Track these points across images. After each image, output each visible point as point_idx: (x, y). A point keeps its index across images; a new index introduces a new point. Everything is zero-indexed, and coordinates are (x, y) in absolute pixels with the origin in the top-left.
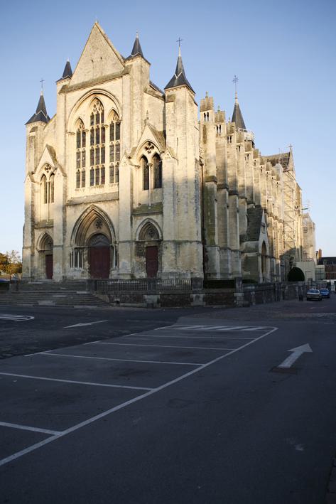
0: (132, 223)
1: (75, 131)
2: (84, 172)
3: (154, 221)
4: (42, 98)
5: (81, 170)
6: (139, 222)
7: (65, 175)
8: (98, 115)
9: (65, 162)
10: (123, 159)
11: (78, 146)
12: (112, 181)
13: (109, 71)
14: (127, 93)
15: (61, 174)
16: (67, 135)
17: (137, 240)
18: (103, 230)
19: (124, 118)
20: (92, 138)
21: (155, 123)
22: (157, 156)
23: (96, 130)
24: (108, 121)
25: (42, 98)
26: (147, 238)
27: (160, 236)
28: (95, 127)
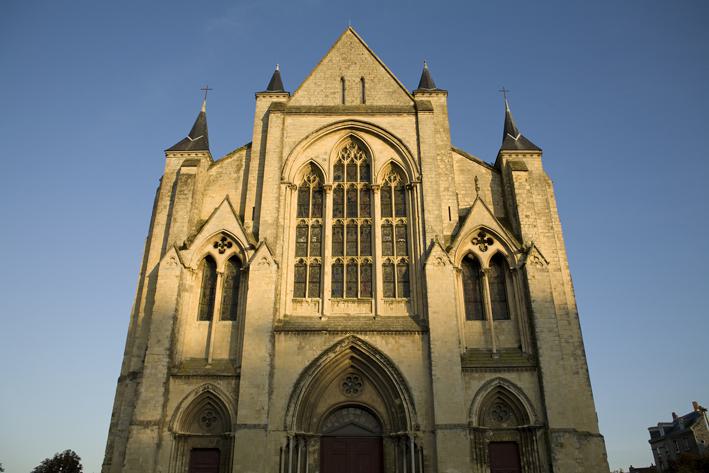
1: (298, 183)
3: (515, 386)
5: (309, 260)
8: (352, 165)
9: (276, 237)
11: (302, 211)
16: (283, 186)
17: (475, 425)
26: (491, 423)
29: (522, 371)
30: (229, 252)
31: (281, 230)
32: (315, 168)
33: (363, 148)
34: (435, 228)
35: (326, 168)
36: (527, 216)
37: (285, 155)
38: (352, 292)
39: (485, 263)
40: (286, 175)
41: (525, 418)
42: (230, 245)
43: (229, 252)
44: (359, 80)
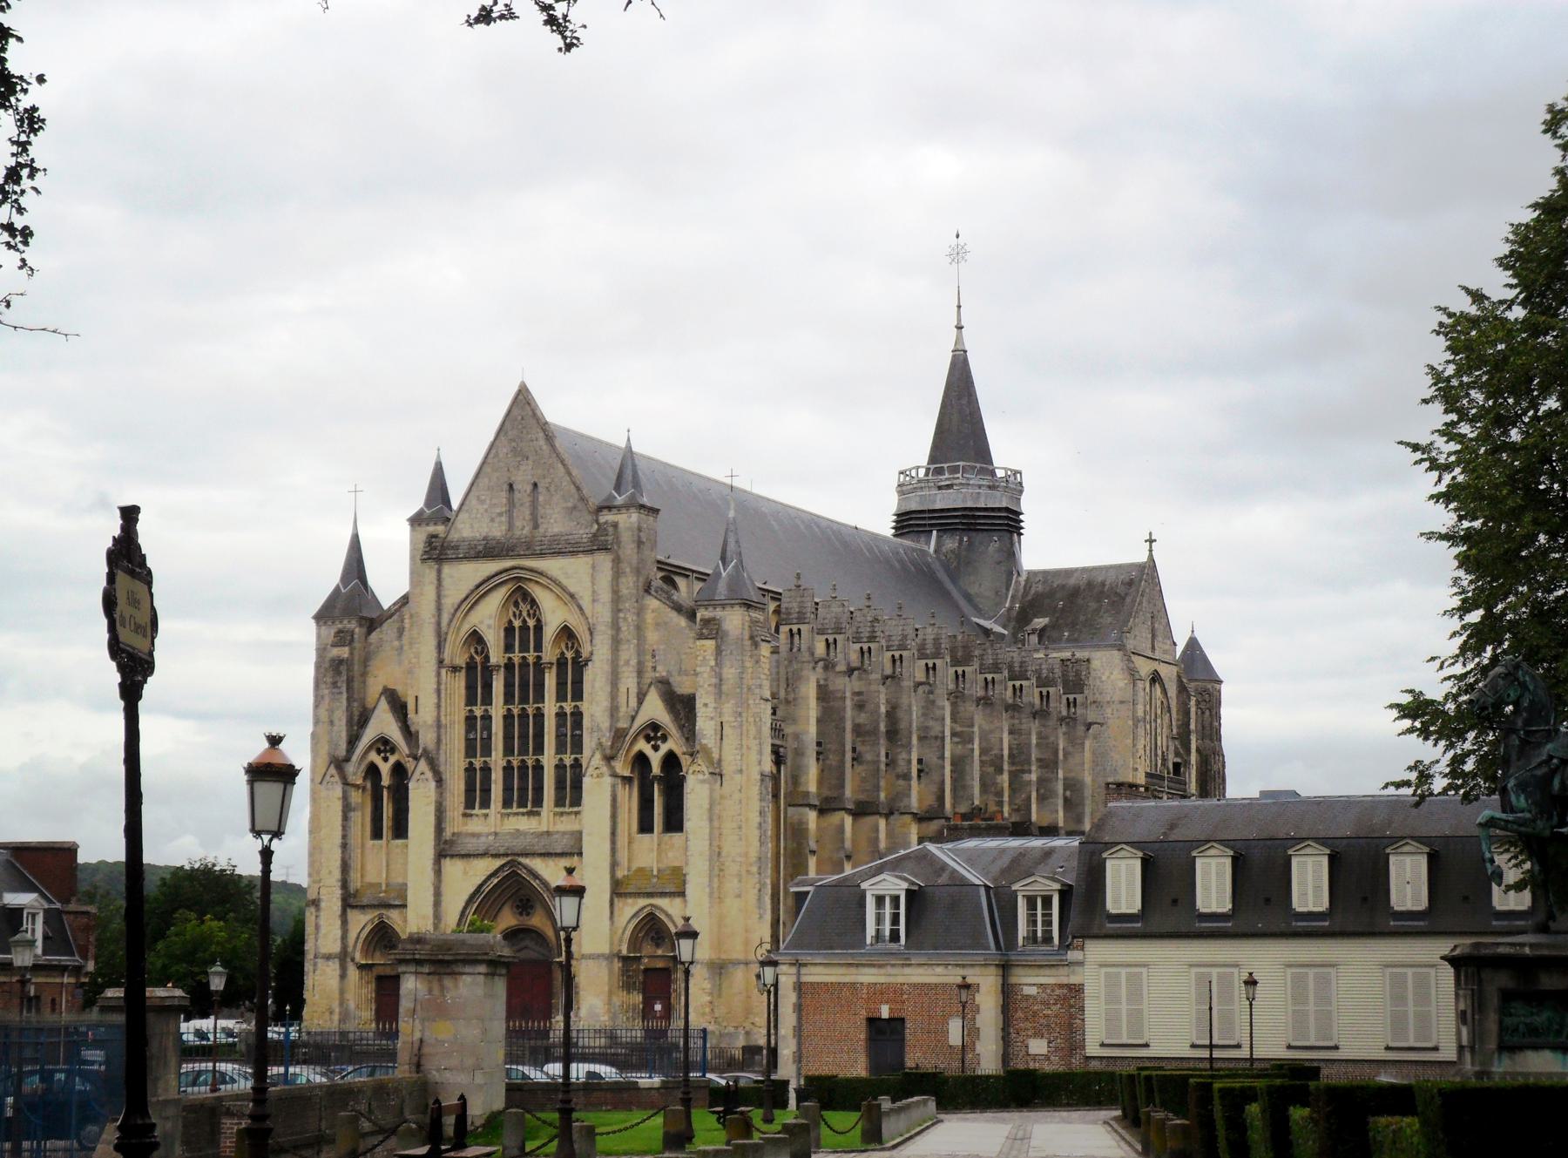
0: (612, 913)
1: (461, 661)
2: (486, 770)
3: (668, 915)
4: (355, 546)
5: (478, 763)
6: (629, 909)
7: (439, 781)
8: (525, 627)
10: (592, 759)
11: (471, 700)
12: (559, 802)
13: (556, 523)
14: (606, 596)
15: (429, 775)
17: (624, 952)
19: (594, 658)
20: (508, 686)
21: (668, 671)
22: (671, 761)
23: (520, 665)
24: (549, 654)
25: (355, 546)
26: (648, 949)
28: (516, 657)
30: (393, 759)
31: (443, 731)
33: (533, 602)
34: (601, 725)
36: (706, 705)
38: (522, 804)
39: (656, 769)
40: (447, 656)
42: (393, 750)
43: (393, 759)
44: (529, 488)
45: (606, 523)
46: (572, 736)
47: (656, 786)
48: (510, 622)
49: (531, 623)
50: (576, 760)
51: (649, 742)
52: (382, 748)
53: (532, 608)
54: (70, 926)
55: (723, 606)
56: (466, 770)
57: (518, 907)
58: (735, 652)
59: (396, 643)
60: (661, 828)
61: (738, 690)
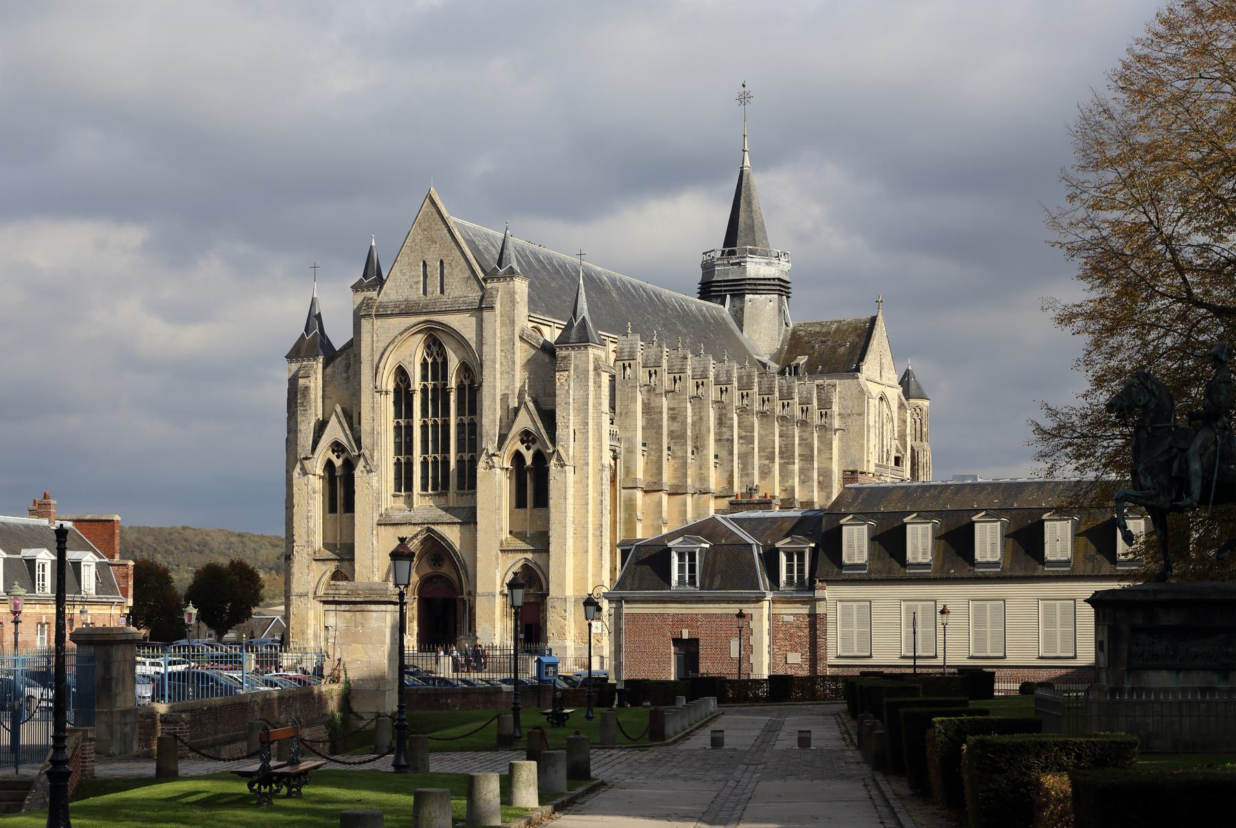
8: (434, 364)
11: (398, 415)
12: (460, 486)
18: (445, 569)
27: (545, 587)
29: (542, 552)
32: (402, 374)
33: (441, 346)
35: (411, 371)
37: (376, 361)
39: (529, 462)
41: (541, 589)
45: (492, 288)
46: (469, 439)
47: (528, 474)
48: (425, 359)
49: (439, 360)
50: (472, 456)
51: (523, 444)
52: (336, 449)
53: (439, 349)
54: (115, 574)
55: (573, 348)
56: (395, 464)
57: (432, 560)
58: (584, 380)
59: (345, 375)
60: (532, 504)
61: (586, 407)
